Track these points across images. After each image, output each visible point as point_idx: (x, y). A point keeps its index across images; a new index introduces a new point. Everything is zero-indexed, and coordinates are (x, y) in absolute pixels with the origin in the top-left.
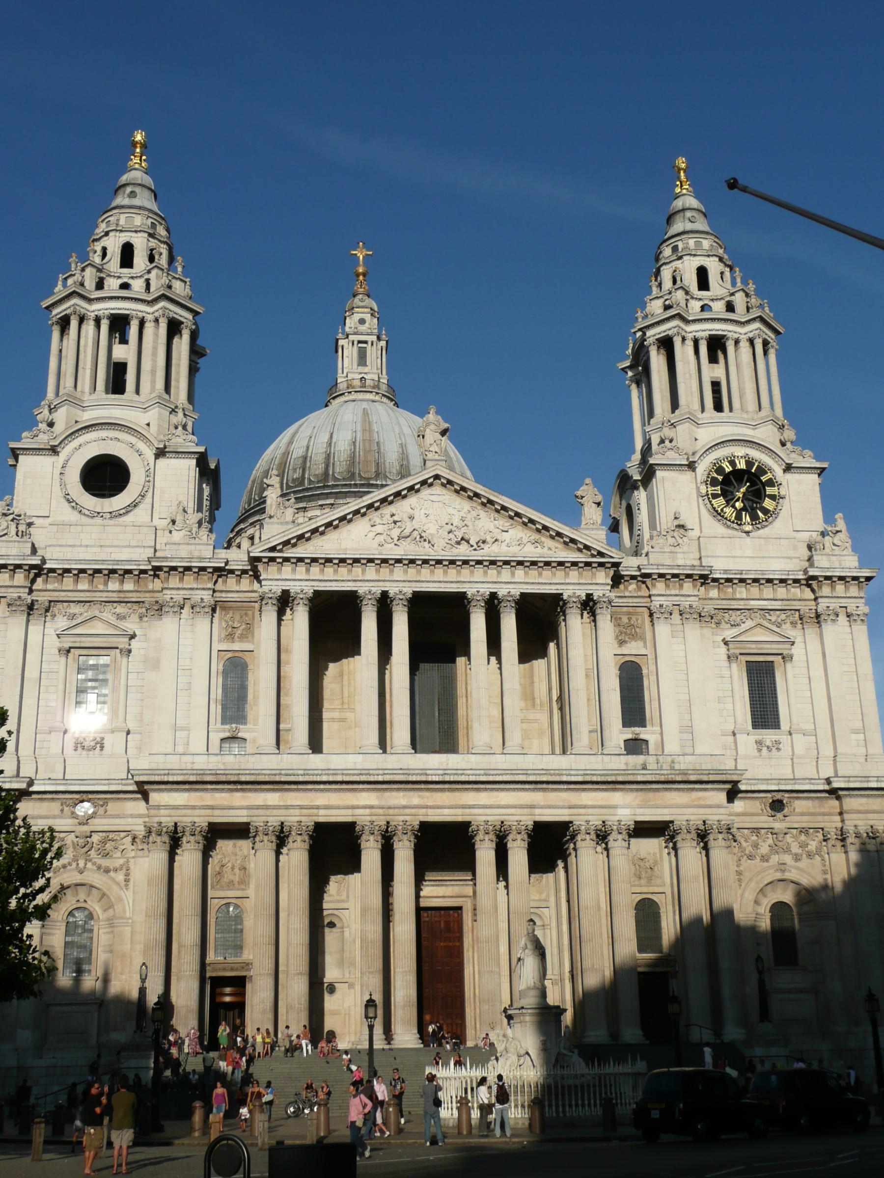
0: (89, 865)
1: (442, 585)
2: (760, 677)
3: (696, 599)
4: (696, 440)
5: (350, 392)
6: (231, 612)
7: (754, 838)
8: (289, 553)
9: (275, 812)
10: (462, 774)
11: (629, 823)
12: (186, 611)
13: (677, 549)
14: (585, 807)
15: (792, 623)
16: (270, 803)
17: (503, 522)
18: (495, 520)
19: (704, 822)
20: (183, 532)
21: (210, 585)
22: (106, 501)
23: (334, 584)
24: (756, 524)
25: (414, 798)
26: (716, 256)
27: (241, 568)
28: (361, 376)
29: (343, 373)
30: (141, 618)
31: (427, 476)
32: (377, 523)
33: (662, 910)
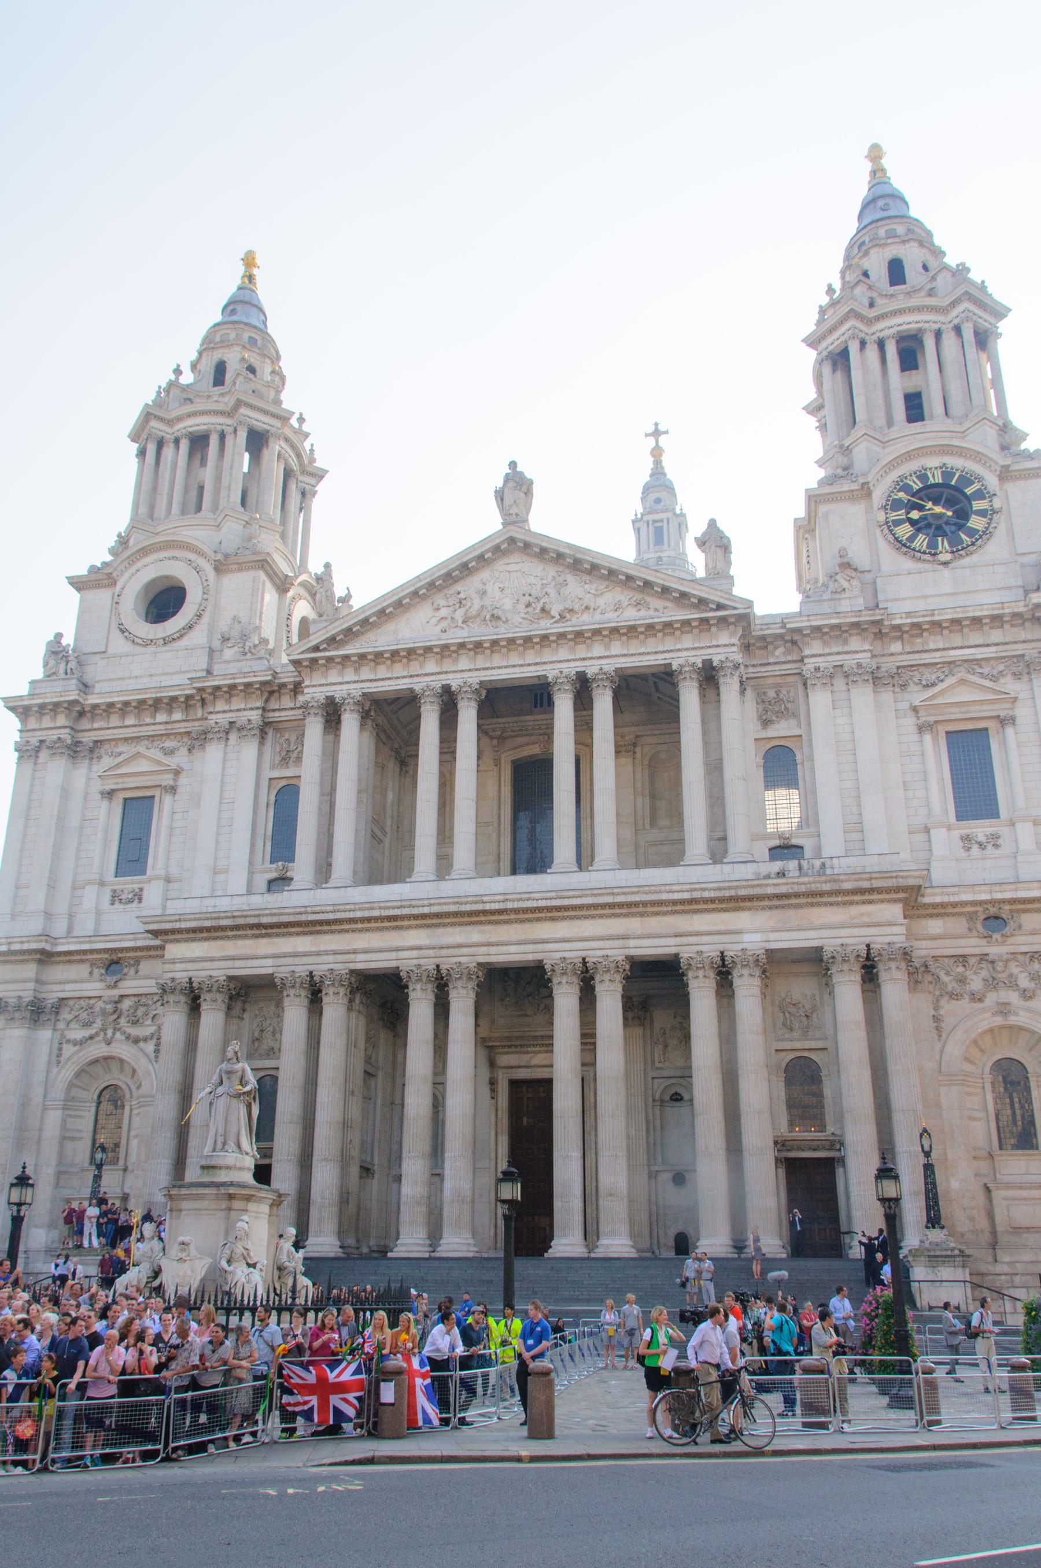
0: (118, 1035)
1: (517, 670)
2: (969, 751)
7: (961, 969)
9: (305, 960)
10: (528, 899)
11: (758, 952)
12: (233, 737)
13: (843, 596)
14: (697, 934)
15: (1014, 674)
16: (300, 949)
19: (868, 946)
20: (236, 648)
21: (259, 704)
22: (159, 627)
23: (387, 683)
24: (958, 550)
25: (474, 934)
26: (914, 240)
27: (292, 679)
30: (190, 750)
33: (824, 1072)
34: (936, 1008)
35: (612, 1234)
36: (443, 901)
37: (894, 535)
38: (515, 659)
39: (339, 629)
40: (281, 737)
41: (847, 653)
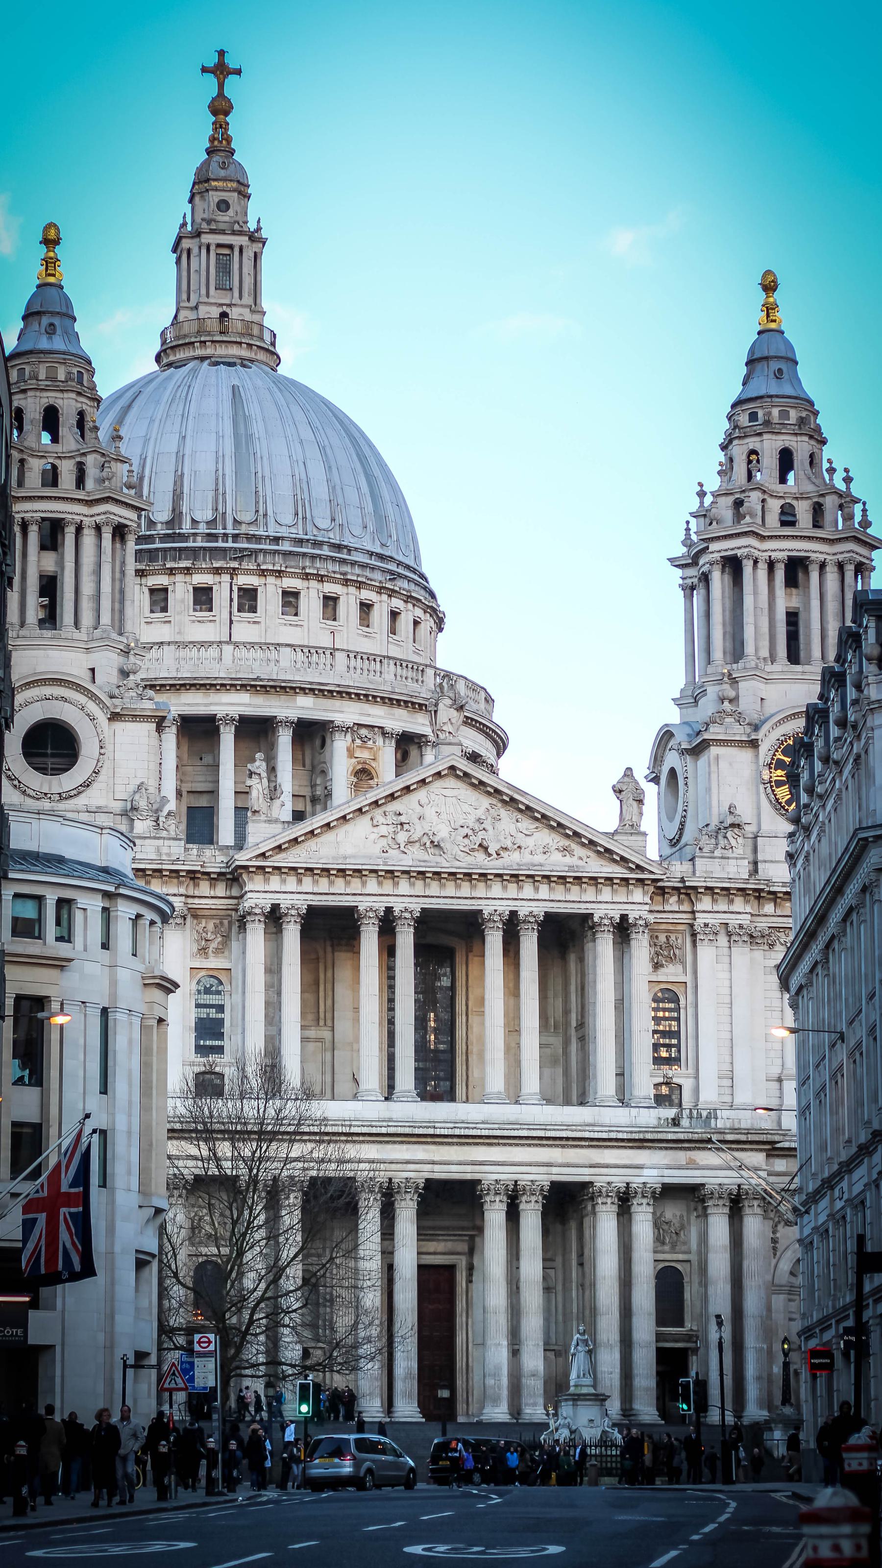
3: (749, 917)
4: (762, 699)
5: (205, 342)
6: (204, 921)
8: (280, 860)
13: (729, 853)
14: (607, 1166)
17: (526, 824)
18: (517, 821)
19: (739, 1186)
21: (182, 890)
25: (419, 1152)
26: (806, 434)
27: (218, 870)
28: (220, 310)
29: (189, 300)
31: (440, 768)
32: (380, 823)
33: (686, 1279)
34: (774, 1232)
35: (535, 1404)
36: (400, 1124)
37: (775, 795)
38: (450, 889)
39: (287, 839)
40: (197, 925)
41: (732, 913)
